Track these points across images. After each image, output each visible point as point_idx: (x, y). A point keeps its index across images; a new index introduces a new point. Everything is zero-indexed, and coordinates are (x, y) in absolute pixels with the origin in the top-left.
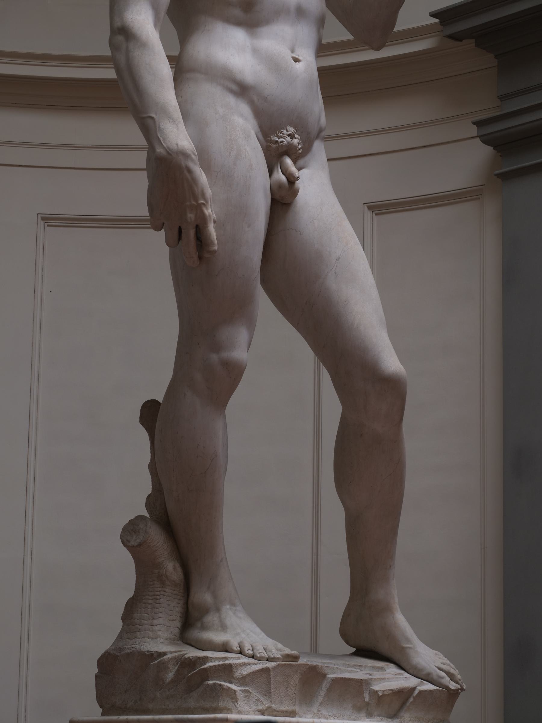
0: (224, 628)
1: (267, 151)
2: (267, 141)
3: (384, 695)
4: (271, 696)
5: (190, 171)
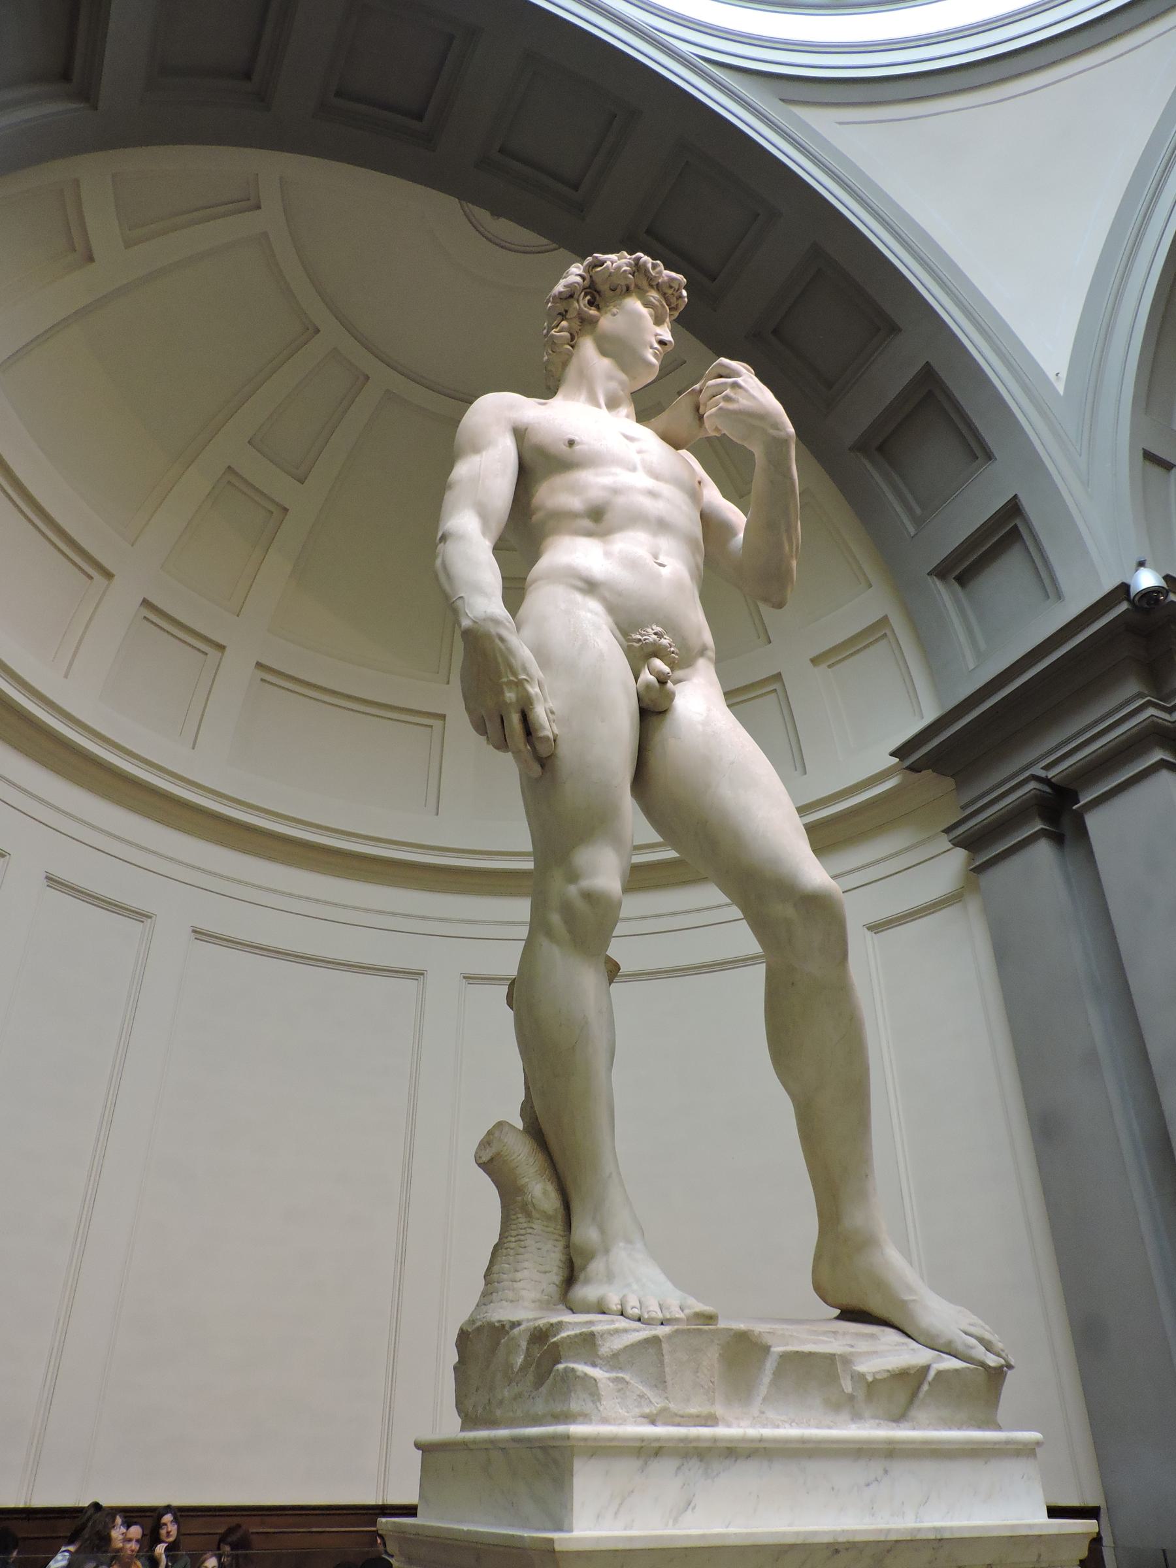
0: (610, 1277)
1: (629, 652)
2: (628, 640)
3: (875, 1381)
4: (665, 1389)
5: (502, 639)
